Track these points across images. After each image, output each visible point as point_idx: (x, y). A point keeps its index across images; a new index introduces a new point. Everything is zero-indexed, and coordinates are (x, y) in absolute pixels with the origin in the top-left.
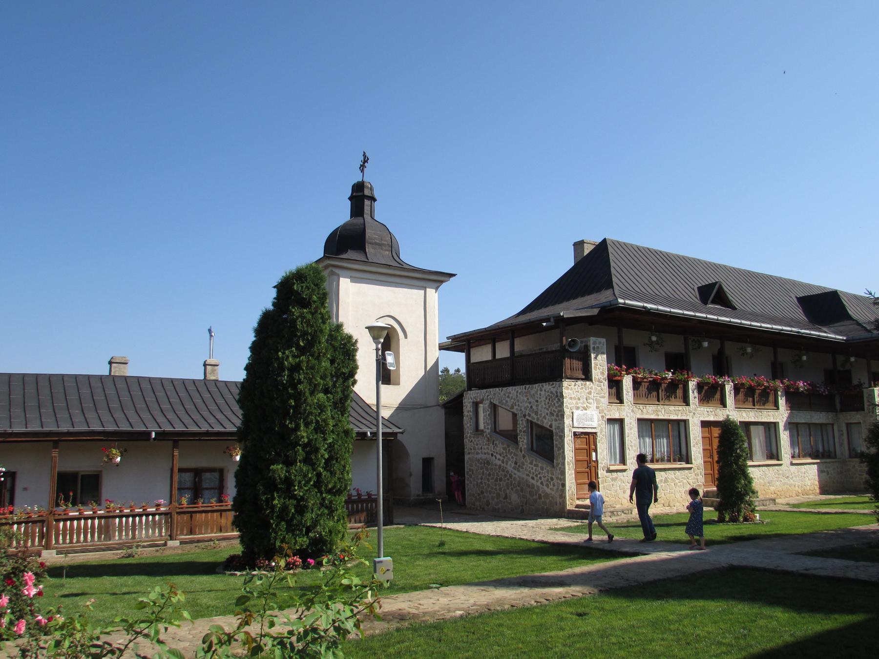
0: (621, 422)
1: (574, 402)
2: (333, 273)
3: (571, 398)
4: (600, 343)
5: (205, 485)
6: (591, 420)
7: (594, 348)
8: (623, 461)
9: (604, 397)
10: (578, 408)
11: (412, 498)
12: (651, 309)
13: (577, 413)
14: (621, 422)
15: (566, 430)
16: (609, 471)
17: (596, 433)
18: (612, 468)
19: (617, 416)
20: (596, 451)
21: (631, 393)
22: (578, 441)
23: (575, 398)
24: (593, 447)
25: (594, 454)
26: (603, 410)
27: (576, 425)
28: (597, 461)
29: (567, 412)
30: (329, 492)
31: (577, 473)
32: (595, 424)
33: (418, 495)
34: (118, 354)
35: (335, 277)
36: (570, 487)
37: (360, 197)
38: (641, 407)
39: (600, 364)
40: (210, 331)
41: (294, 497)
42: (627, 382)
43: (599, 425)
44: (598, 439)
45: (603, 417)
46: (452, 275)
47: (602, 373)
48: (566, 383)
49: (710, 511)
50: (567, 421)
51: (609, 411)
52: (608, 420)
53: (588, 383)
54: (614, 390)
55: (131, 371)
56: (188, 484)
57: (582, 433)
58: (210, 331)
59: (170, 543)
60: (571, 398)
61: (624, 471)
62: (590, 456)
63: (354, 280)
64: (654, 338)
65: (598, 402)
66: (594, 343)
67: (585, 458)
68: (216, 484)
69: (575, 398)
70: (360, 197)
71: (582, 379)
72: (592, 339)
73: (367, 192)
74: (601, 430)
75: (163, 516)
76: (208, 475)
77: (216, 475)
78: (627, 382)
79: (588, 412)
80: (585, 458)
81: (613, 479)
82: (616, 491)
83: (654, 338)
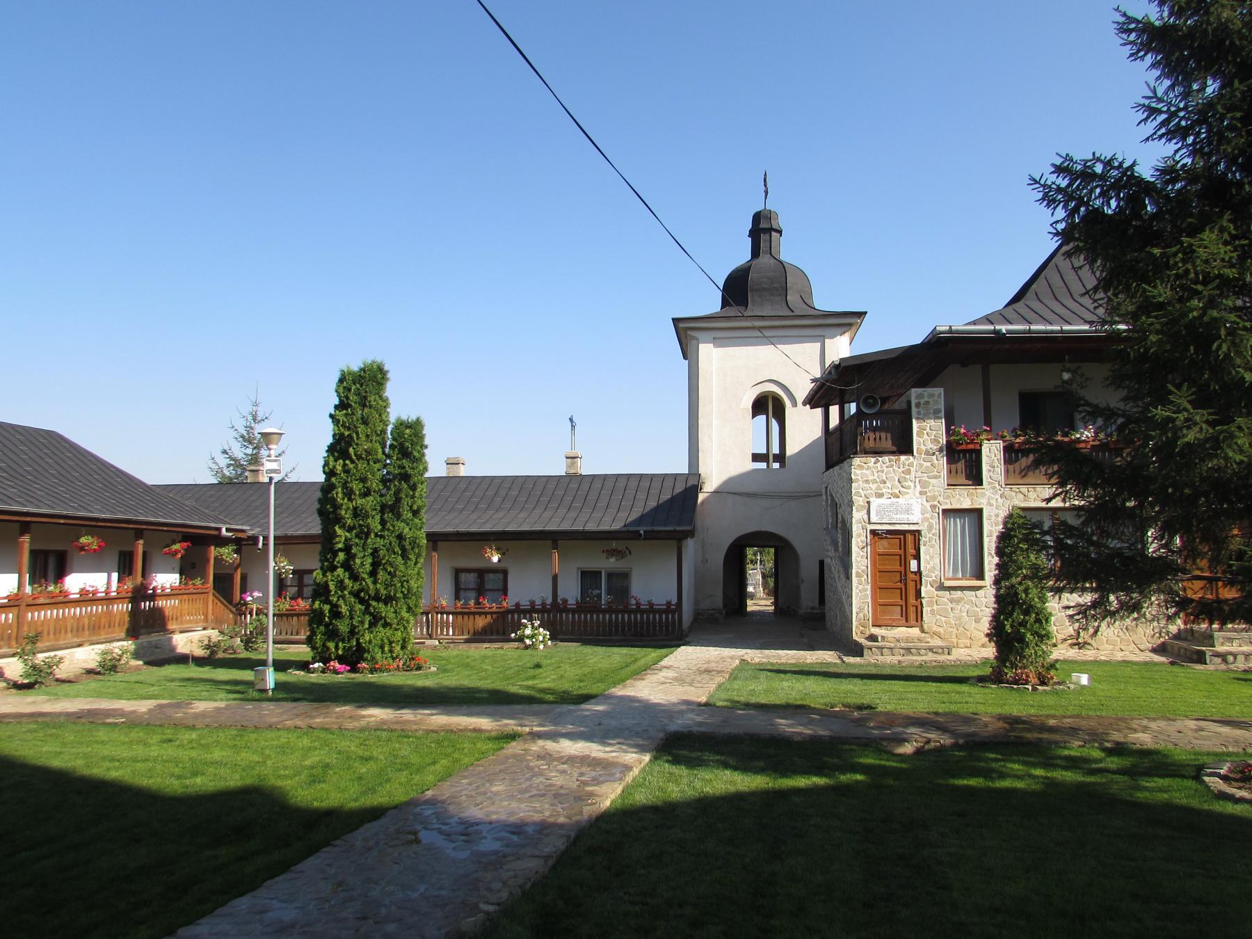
0: (978, 513)
1: (874, 486)
2: (693, 338)
3: (867, 481)
4: (932, 396)
5: (488, 586)
6: (908, 511)
7: (918, 405)
8: (980, 575)
9: (936, 477)
10: (880, 495)
11: (801, 612)
12: (1009, 332)
13: (875, 503)
14: (978, 513)
15: (856, 529)
16: (942, 587)
17: (919, 532)
18: (947, 583)
19: (966, 504)
20: (917, 557)
21: (1000, 468)
22: (885, 542)
23: (874, 481)
24: (911, 551)
25: (913, 564)
26: (934, 498)
27: (873, 519)
28: (919, 573)
29: (858, 501)
30: (377, 598)
31: (879, 589)
32: (916, 516)
33: (813, 608)
34: (452, 455)
35: (694, 342)
36: (861, 609)
37: (762, 230)
38: (1024, 489)
39: (929, 433)
40: (571, 420)
41: (329, 602)
42: (992, 453)
43: (925, 520)
44: (923, 540)
45: (933, 507)
46: (861, 315)
47: (935, 441)
48: (857, 461)
49: (1162, 664)
50: (858, 516)
51: (948, 497)
52: (945, 511)
53: (903, 458)
54: (961, 465)
55: (463, 471)
56: (473, 586)
57: (889, 532)
58: (571, 420)
59: (429, 642)
60: (867, 481)
61: (979, 588)
62: (906, 565)
63: (718, 342)
64: (1066, 376)
65: (923, 484)
66: (919, 396)
67: (898, 568)
68: (500, 586)
69: (874, 481)
70: (762, 230)
71: (892, 453)
72: (914, 392)
73: (763, 225)
74: (930, 527)
75: (460, 617)
76: (491, 576)
77: (501, 576)
78: (992, 453)
79: (901, 500)
80: (898, 568)
81: (958, 601)
82: (959, 618)
83: (1066, 376)
